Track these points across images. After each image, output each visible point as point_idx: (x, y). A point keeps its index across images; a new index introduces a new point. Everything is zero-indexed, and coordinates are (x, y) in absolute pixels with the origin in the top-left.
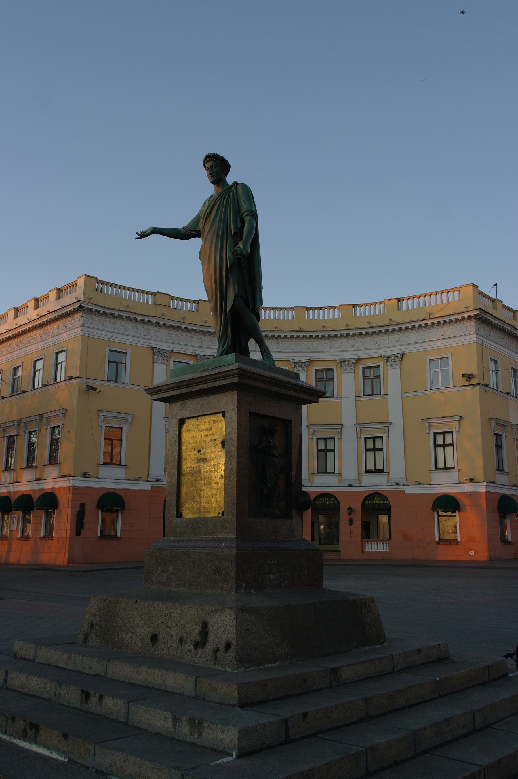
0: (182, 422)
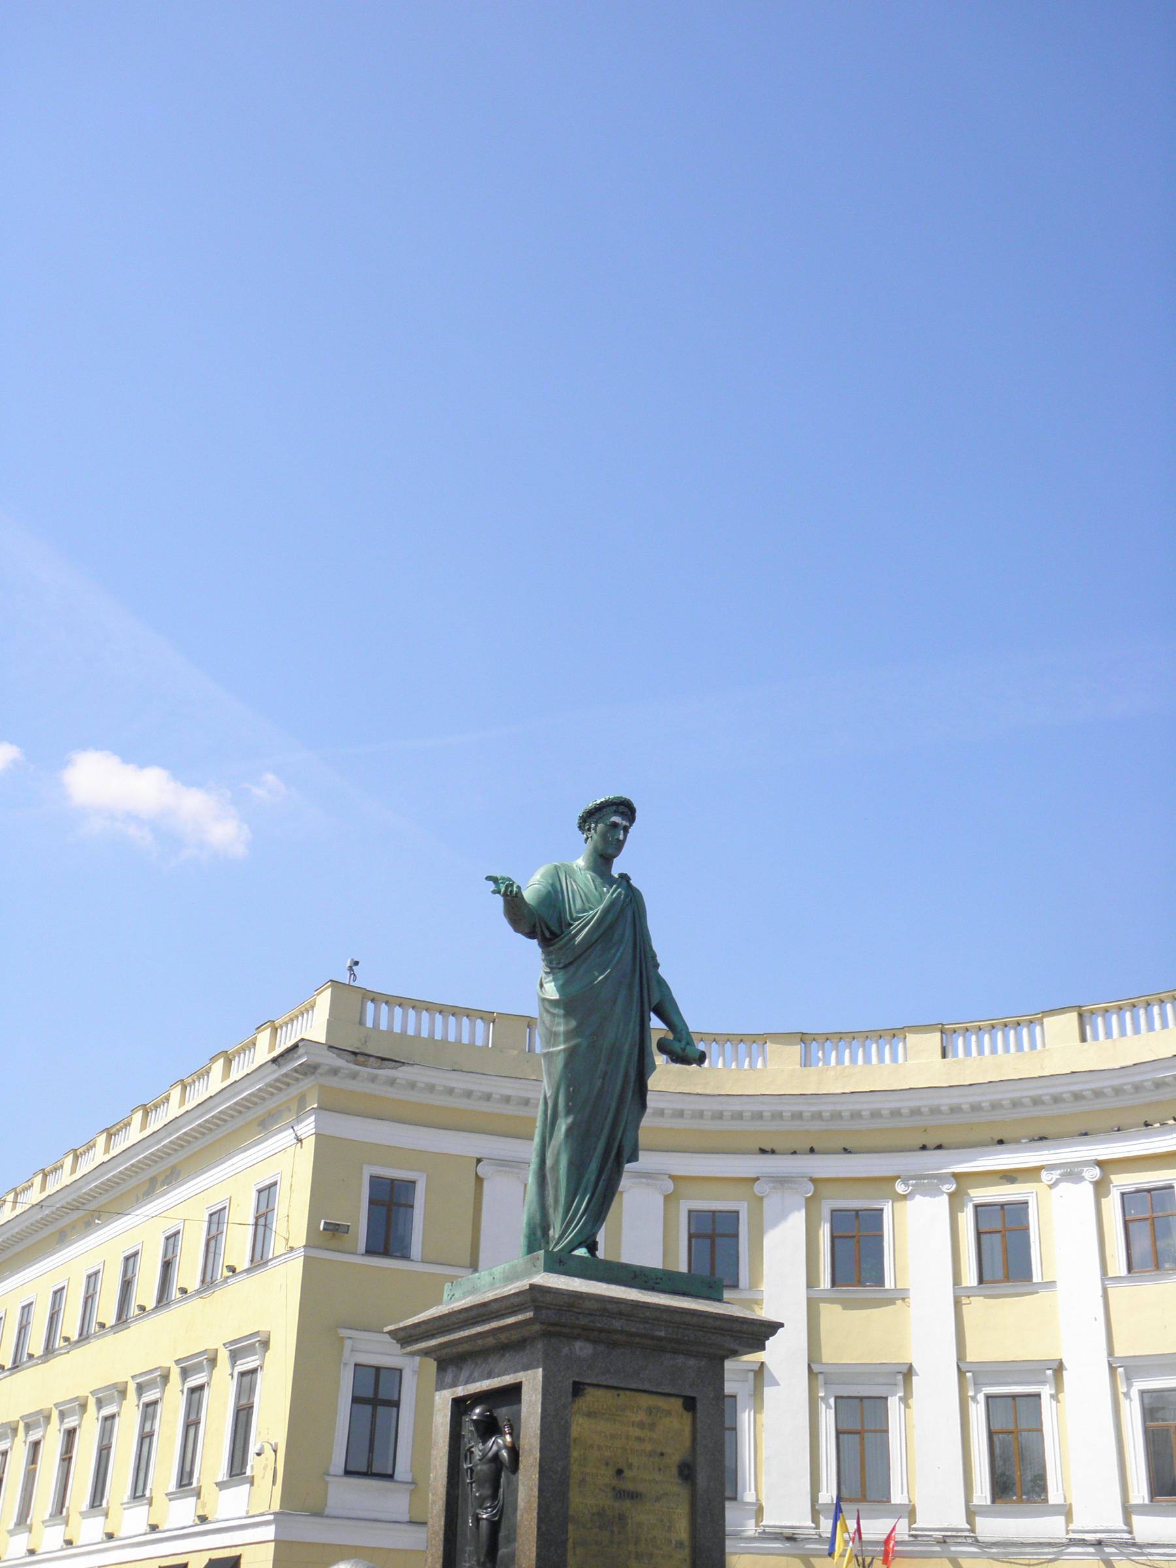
0: (578, 1389)
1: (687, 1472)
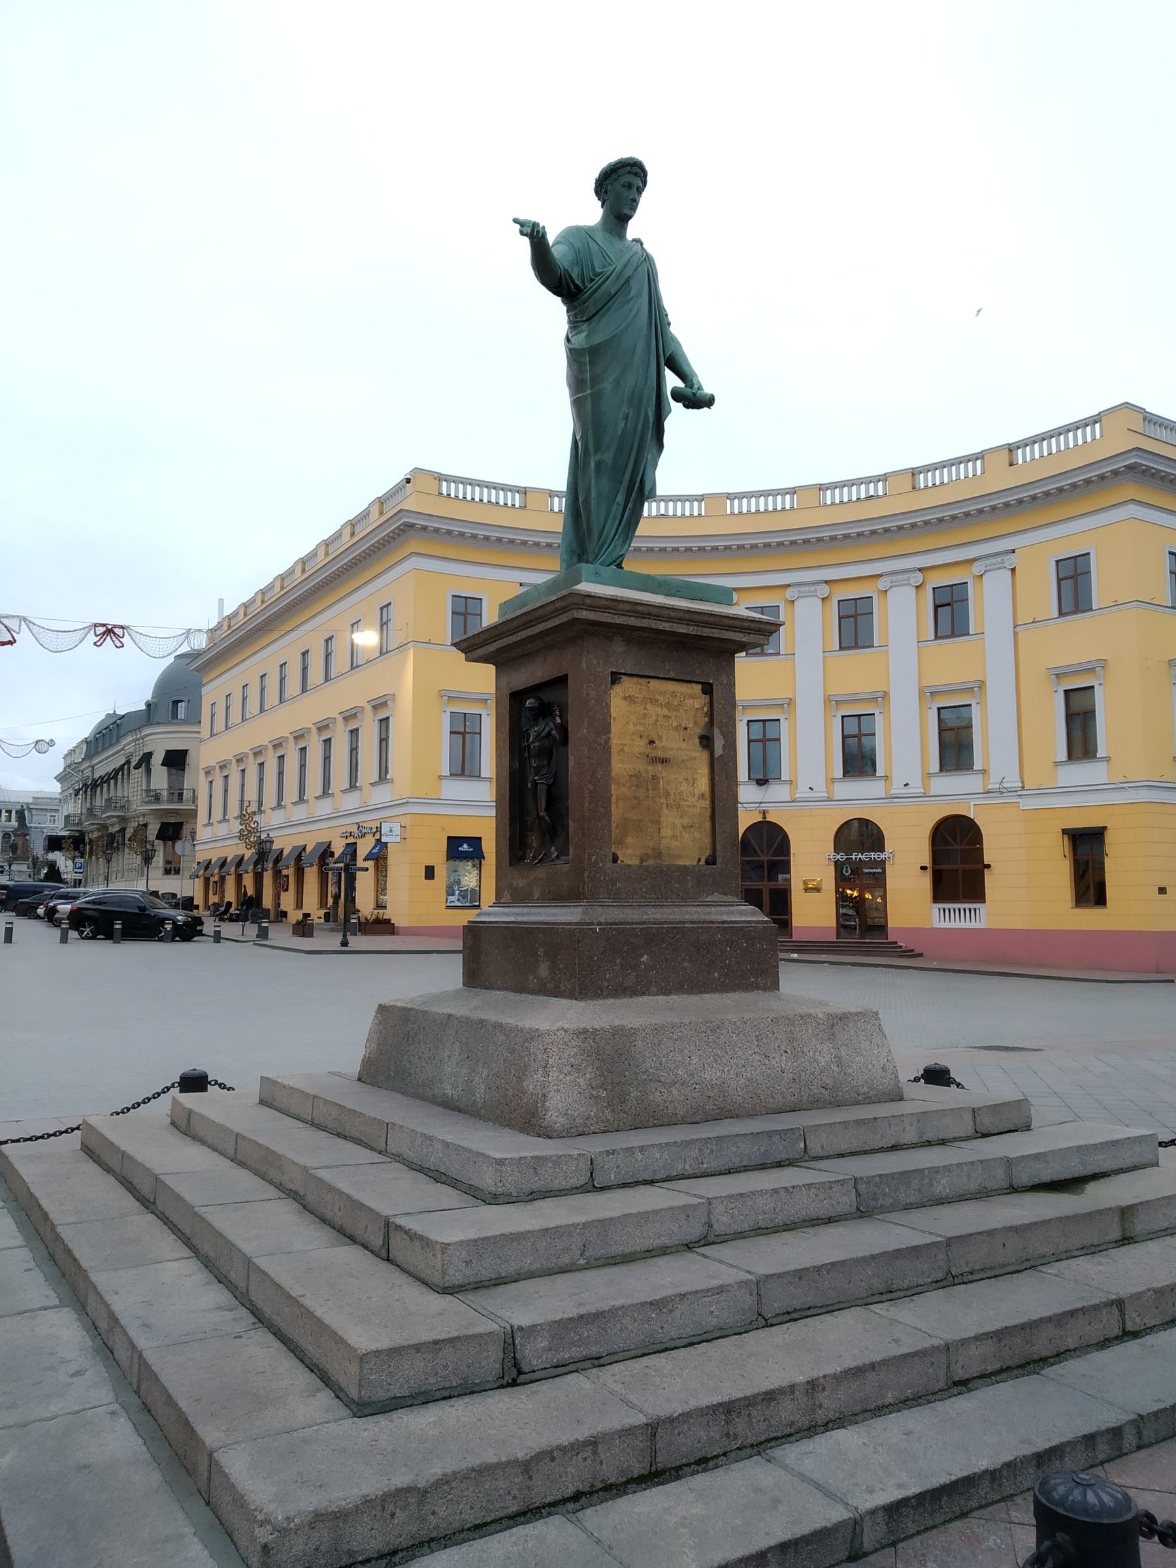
0: (615, 678)
1: (706, 741)
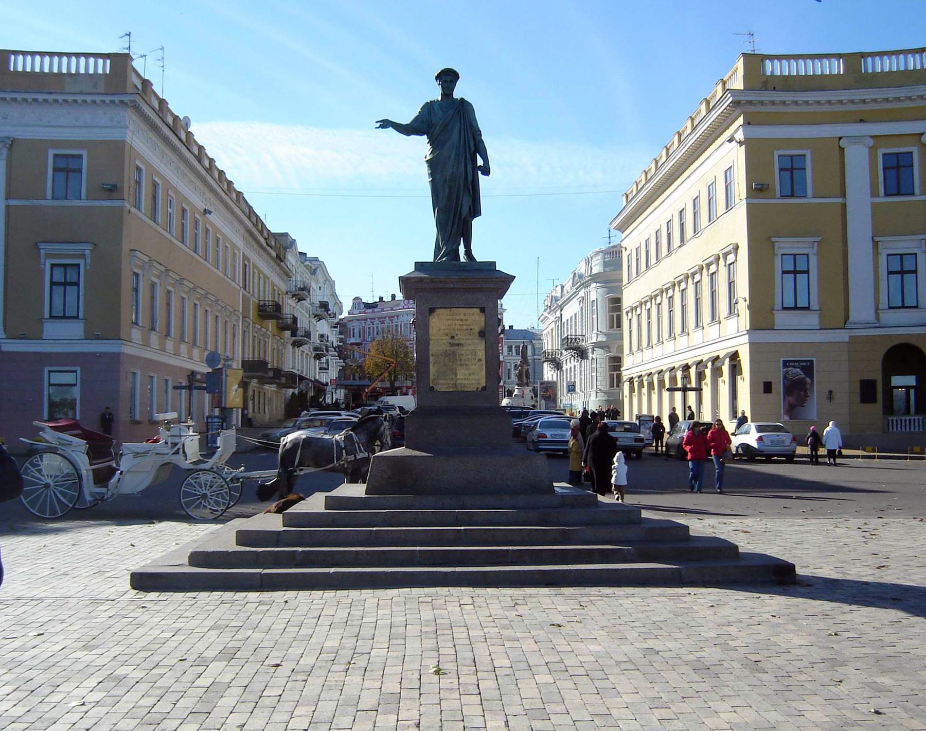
0: (432, 311)
1: (482, 334)
